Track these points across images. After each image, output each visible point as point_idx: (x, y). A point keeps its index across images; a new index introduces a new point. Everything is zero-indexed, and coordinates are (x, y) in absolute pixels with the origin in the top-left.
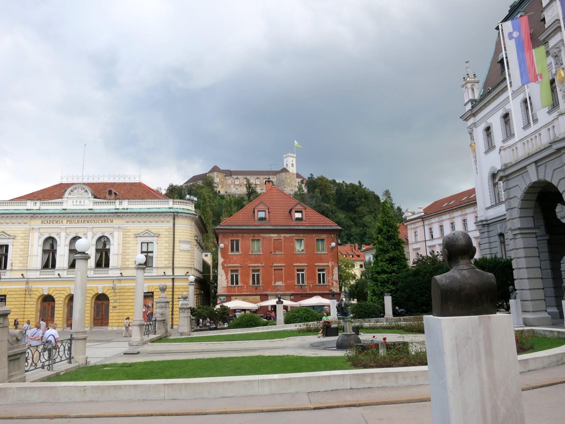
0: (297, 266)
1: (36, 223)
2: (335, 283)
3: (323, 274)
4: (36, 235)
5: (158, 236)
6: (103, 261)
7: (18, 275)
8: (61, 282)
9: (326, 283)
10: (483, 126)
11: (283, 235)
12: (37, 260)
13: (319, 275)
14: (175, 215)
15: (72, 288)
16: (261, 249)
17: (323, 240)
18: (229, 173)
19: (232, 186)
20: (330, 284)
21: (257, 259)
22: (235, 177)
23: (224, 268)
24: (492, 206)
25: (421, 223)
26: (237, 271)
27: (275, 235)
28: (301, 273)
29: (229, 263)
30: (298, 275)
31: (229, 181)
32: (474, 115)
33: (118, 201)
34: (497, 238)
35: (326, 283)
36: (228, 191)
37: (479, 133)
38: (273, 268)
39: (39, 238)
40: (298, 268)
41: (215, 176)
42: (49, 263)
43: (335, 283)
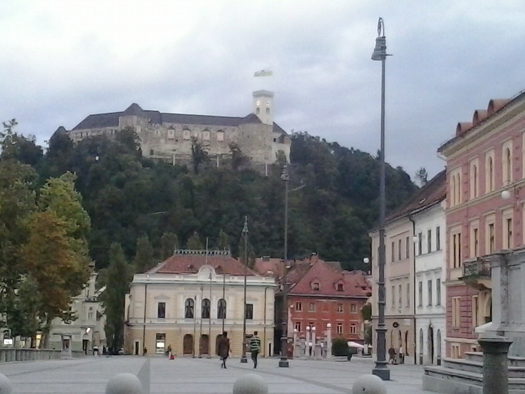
1: (182, 289)
4: (182, 296)
5: (256, 300)
6: (222, 314)
7: (173, 322)
8: (197, 327)
9: (356, 333)
12: (182, 313)
13: (352, 328)
14: (267, 287)
15: (205, 332)
16: (315, 309)
18: (157, 118)
19: (162, 141)
20: (358, 334)
21: (313, 315)
22: (168, 125)
23: (292, 320)
26: (300, 323)
29: (295, 317)
31: (158, 131)
33: (231, 277)
35: (356, 333)
36: (155, 149)
39: (184, 299)
41: (135, 123)
42: (189, 315)
43: (362, 334)
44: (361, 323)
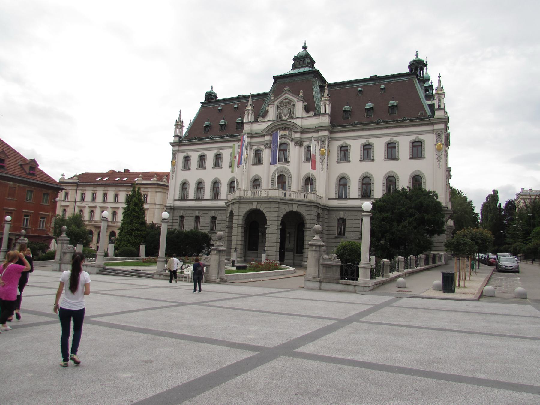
0: (25, 212)
2: (51, 229)
3: (27, 219)
10: (185, 154)
11: (18, 184)
17: (48, 194)
24: (179, 200)
25: (75, 188)
27: (12, 183)
28: (26, 218)
30: (24, 219)
32: (179, 145)
34: (178, 218)
37: (180, 157)
38: (5, 211)
40: (26, 214)
43: (51, 229)
44: (52, 217)
